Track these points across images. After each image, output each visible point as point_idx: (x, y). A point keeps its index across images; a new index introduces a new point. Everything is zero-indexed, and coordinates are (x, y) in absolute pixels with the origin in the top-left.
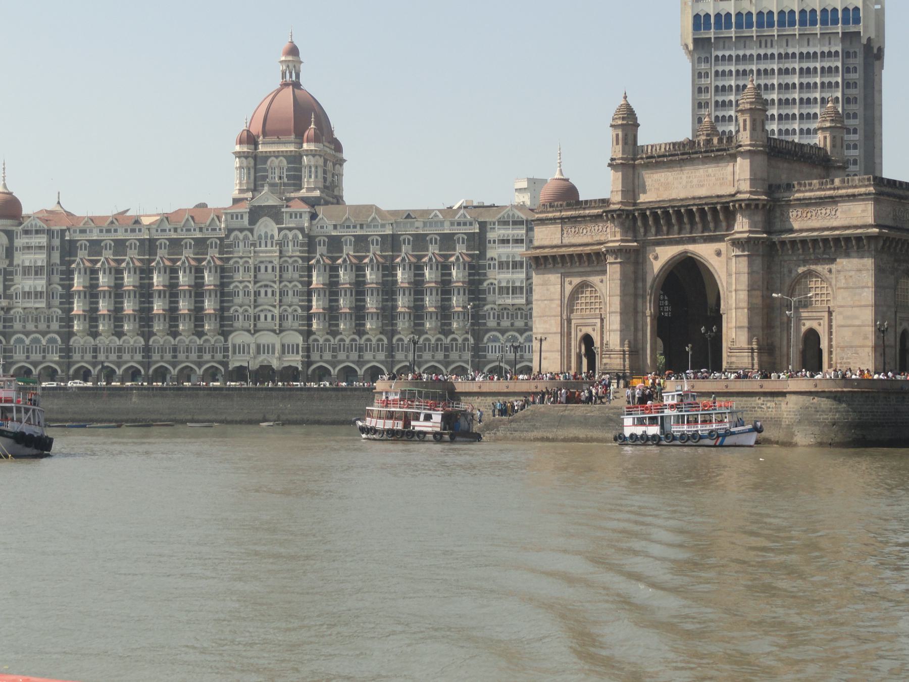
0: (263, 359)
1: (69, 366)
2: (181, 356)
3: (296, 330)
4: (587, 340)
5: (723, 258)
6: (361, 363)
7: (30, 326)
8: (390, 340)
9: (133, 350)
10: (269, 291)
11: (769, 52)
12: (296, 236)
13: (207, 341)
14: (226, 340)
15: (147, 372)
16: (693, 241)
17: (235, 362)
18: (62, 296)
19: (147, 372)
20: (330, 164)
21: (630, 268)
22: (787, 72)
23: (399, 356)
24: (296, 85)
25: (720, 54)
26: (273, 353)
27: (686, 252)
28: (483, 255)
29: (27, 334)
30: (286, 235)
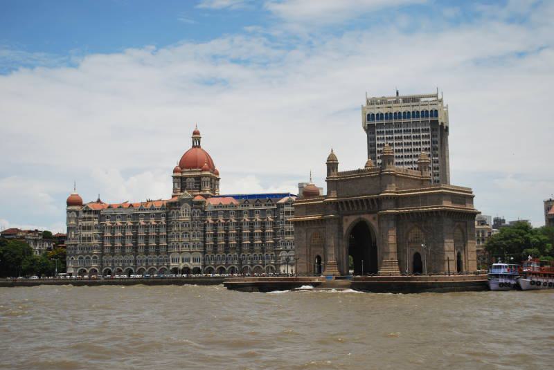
1: (101, 269)
2: (150, 264)
5: (377, 221)
9: (129, 261)
10: (187, 235)
12: (198, 211)
13: (161, 257)
15: (135, 270)
16: (363, 214)
17: (173, 265)
19: (135, 270)
20: (213, 181)
21: (335, 226)
24: (199, 147)
25: (379, 130)
27: (360, 218)
29: (84, 255)
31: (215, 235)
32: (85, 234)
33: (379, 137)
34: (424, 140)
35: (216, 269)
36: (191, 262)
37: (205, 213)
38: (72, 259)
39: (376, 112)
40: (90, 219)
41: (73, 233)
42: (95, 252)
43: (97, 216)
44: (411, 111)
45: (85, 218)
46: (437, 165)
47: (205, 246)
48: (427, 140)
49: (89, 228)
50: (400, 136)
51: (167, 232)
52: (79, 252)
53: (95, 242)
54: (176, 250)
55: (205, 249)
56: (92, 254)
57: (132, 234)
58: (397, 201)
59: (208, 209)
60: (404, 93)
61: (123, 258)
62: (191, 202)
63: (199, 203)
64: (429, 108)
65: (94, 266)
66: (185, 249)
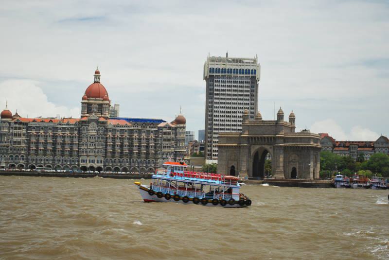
0: (92, 164)
1: (27, 164)
3: (102, 156)
4: (233, 167)
5: (272, 149)
6: (121, 166)
7: (15, 152)
8: (130, 160)
10: (94, 144)
11: (230, 80)
12: (102, 129)
14: (79, 158)
16: (264, 145)
17: (82, 164)
18: (26, 143)
21: (247, 150)
22: (235, 86)
23: (132, 164)
25: (217, 80)
26: (94, 162)
27: (262, 147)
28: (158, 136)
29: (14, 154)
30: (99, 128)
31: (114, 146)
32: (15, 139)
33: (216, 84)
34: (247, 89)
35: (113, 169)
36: (96, 163)
37: (107, 130)
38: (5, 156)
39: (215, 67)
40: (20, 128)
41: (6, 138)
42: (23, 152)
43: (25, 127)
44: (239, 69)
45: (17, 128)
46: (253, 106)
47: (106, 153)
48: (248, 89)
49: (20, 135)
50: (230, 85)
51: (79, 142)
52: (10, 152)
53: (23, 145)
54: (85, 154)
55: (106, 155)
56: (20, 154)
57: (52, 141)
58: (285, 140)
59: (109, 127)
60: (231, 56)
61: (44, 158)
62: (97, 121)
63: (103, 123)
64: (251, 68)
65: (22, 162)
66: (91, 154)
